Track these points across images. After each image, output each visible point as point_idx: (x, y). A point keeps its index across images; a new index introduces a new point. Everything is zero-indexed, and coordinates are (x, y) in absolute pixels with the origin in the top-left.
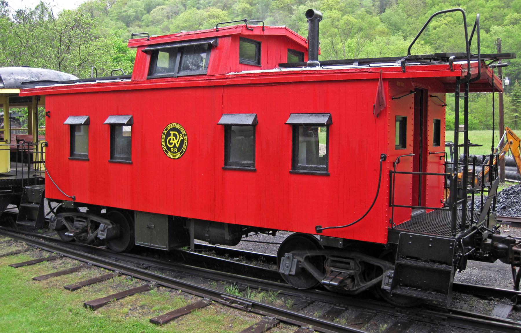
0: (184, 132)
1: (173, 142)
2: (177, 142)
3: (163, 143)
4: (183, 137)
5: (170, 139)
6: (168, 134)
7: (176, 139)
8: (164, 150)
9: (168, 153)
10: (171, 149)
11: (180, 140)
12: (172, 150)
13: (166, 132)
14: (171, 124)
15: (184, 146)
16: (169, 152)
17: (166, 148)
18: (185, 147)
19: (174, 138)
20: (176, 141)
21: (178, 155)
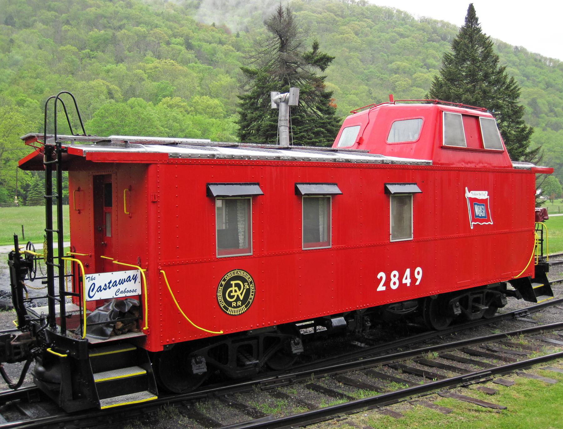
0: (251, 279)
1: (236, 294)
2: (241, 294)
3: (220, 298)
4: (249, 286)
5: (231, 291)
6: (228, 285)
7: (240, 290)
8: (222, 306)
9: (227, 309)
11: (245, 290)
12: (234, 304)
13: (223, 283)
14: (232, 272)
15: (251, 296)
16: (230, 308)
17: (224, 304)
18: (253, 297)
19: (237, 288)
20: (239, 293)
21: (243, 309)
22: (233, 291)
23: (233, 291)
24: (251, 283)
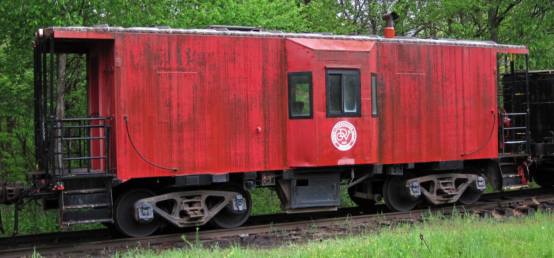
1: (342, 137)
7: (345, 134)
11: (348, 135)
15: (353, 139)
19: (343, 133)
20: (344, 136)
22: (341, 135)
23: (341, 135)
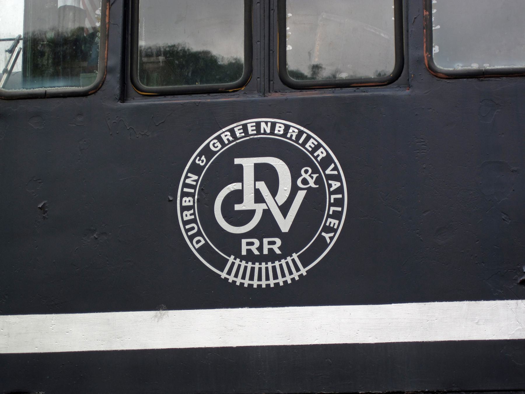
2: (285, 209)
10: (244, 241)
19: (262, 186)
24: (326, 162)
